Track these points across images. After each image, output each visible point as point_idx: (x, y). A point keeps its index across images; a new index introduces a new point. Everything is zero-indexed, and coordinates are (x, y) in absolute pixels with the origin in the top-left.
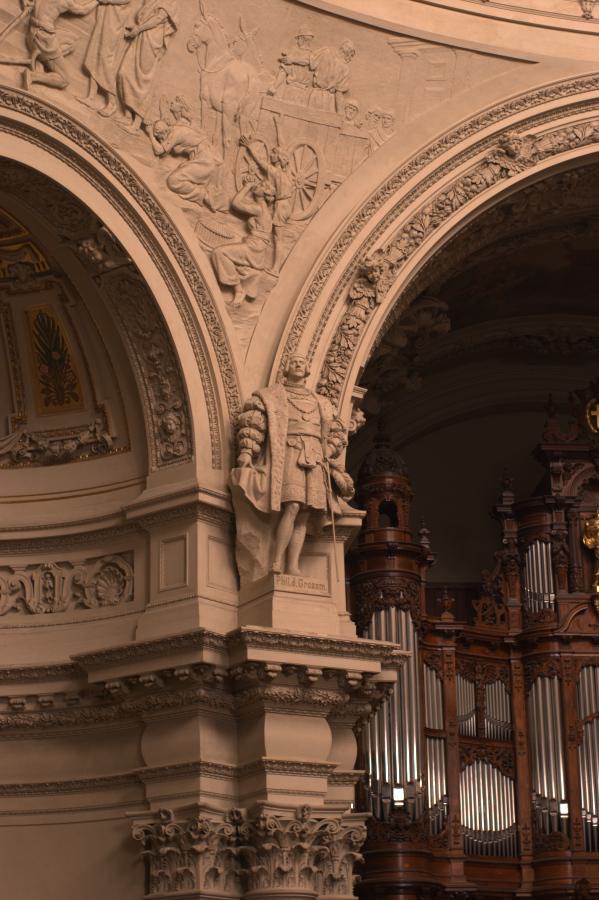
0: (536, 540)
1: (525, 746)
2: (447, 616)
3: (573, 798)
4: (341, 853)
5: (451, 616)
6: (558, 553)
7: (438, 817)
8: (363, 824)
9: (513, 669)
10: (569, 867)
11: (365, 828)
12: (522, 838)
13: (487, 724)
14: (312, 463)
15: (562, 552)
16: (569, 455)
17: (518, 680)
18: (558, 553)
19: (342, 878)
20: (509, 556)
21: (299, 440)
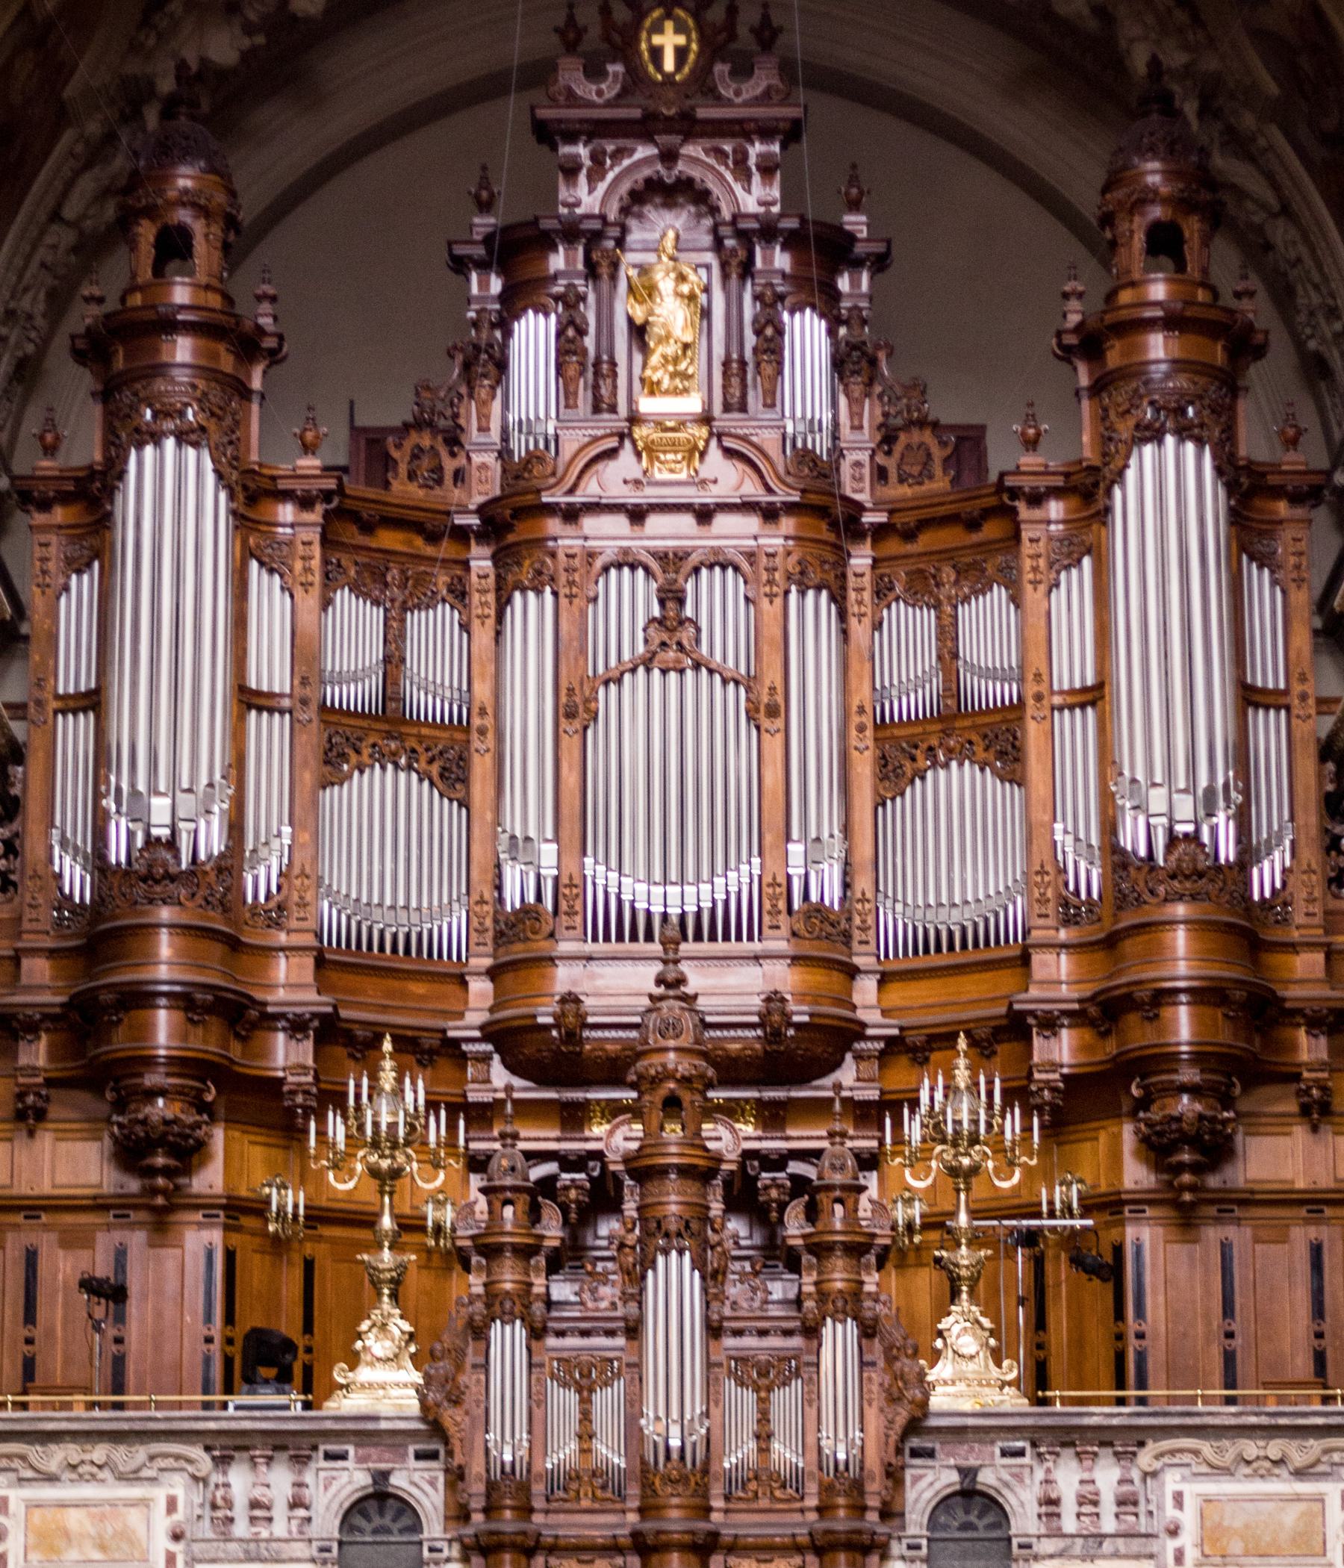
0: (524, 310)
1: (490, 735)
16: (596, 130)
17: (483, 601)
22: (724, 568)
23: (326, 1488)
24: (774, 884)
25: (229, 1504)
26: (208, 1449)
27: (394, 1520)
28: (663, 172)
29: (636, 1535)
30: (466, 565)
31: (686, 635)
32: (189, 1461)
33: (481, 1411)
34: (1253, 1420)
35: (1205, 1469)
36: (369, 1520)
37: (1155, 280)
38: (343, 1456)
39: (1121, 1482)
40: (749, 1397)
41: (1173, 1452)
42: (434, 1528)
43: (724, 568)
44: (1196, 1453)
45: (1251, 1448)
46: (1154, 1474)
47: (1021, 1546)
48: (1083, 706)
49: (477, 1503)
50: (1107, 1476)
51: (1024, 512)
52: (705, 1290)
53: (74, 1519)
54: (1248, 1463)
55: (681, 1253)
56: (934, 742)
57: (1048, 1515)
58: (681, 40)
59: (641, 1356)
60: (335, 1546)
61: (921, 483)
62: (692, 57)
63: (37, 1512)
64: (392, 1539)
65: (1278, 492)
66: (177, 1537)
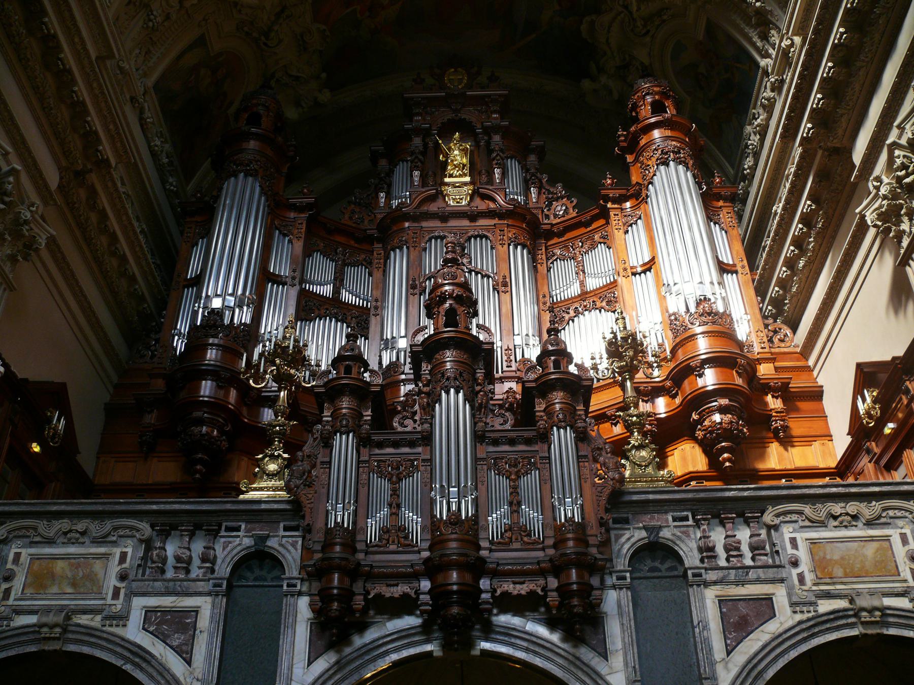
22: (481, 239)
23: (224, 549)
24: (508, 349)
25: (164, 560)
26: (152, 526)
29: (427, 561)
33: (325, 491)
35: (807, 523)
36: (253, 572)
38: (238, 529)
39: (751, 537)
40: (505, 482)
41: (785, 513)
42: (293, 570)
43: (481, 239)
44: (800, 513)
45: (837, 508)
46: (776, 527)
47: (694, 575)
48: (644, 272)
50: (744, 535)
51: (609, 205)
52: (473, 416)
53: (60, 565)
54: (835, 518)
55: (457, 392)
57: (708, 557)
59: (431, 456)
60: (225, 583)
61: (564, 216)
63: (38, 562)
64: (266, 583)
65: (718, 197)
66: (123, 577)
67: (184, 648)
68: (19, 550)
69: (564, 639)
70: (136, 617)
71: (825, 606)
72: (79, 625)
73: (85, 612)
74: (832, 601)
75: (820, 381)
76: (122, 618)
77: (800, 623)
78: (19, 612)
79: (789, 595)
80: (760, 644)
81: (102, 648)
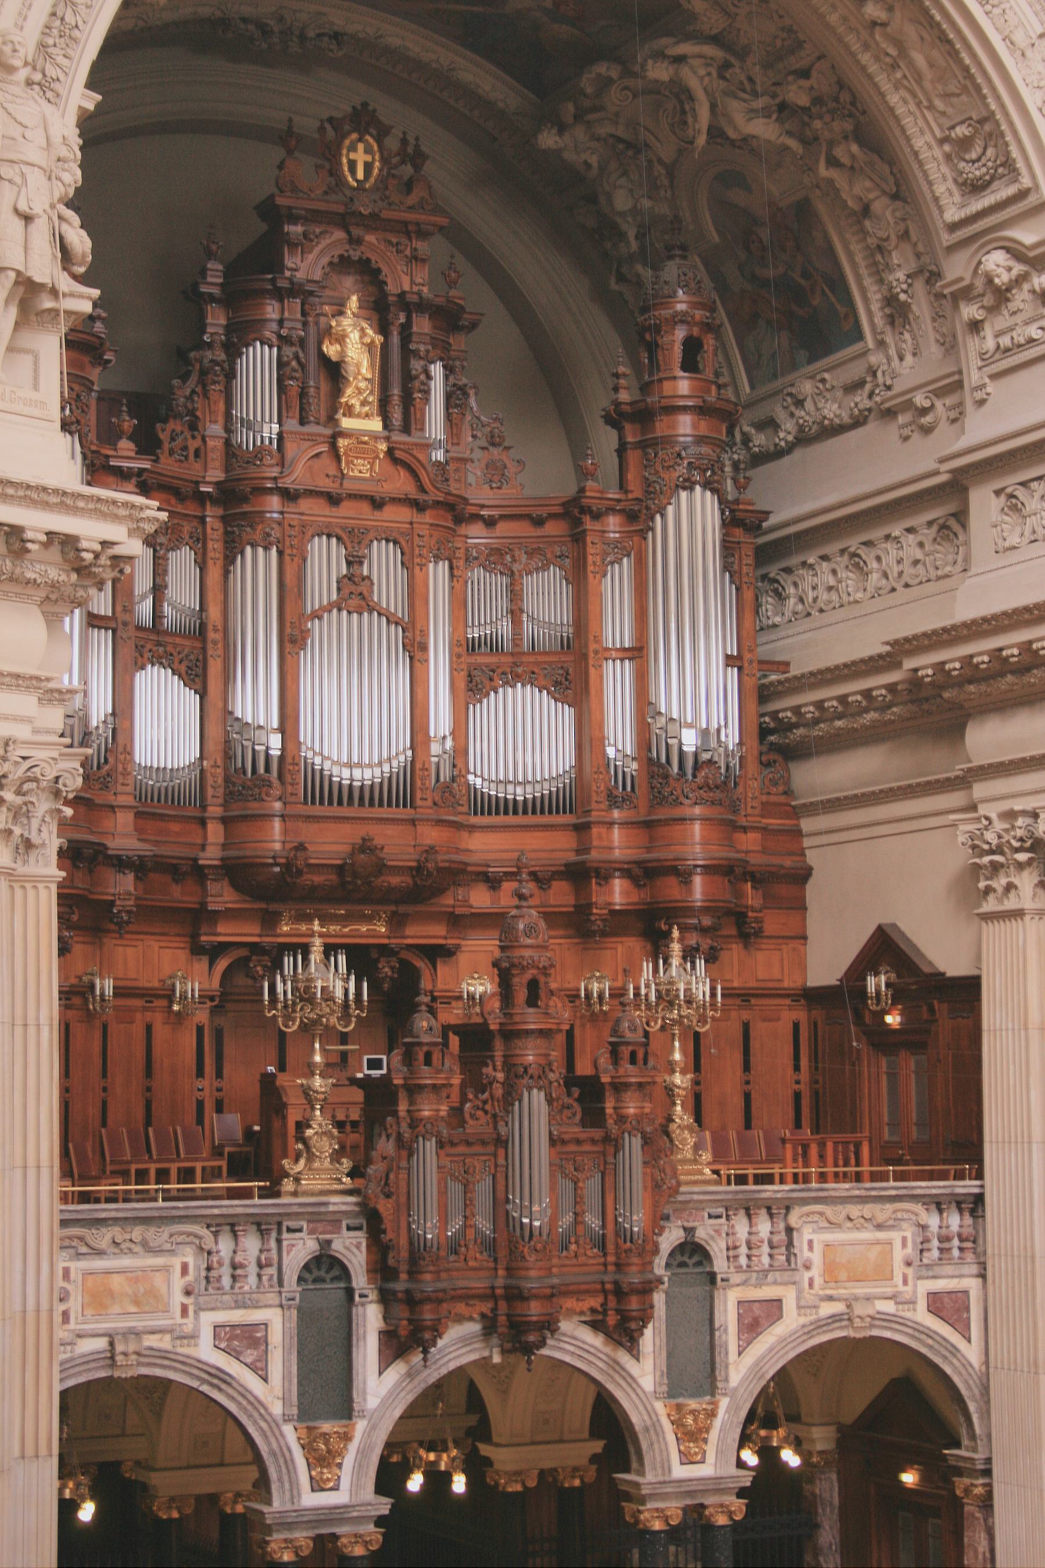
0: (254, 340)
1: (220, 645)
2: (126, 446)
3: (288, 724)
4: (43, 805)
5: (131, 445)
6: (288, 364)
7: (99, 746)
8: (77, 765)
9: (209, 531)
10: (277, 824)
11: (81, 771)
12: (210, 781)
13: (167, 609)
14: (37, 209)
15: (294, 363)
16: (314, 217)
17: (215, 547)
18: (288, 364)
19: (43, 845)
20: (212, 361)
21: (17, 170)
26: (208, 1226)
27: (327, 1272)
28: (351, 252)
30: (202, 520)
31: (363, 588)
32: (196, 1236)
34: (857, 1193)
37: (683, 378)
38: (300, 1230)
41: (808, 1215)
42: (360, 1280)
44: (821, 1214)
45: (855, 1210)
47: (723, 1280)
49: (404, 1267)
50: (764, 1227)
51: (589, 524)
56: (508, 670)
58: (369, 158)
62: (376, 171)
66: (188, 1293)
67: (259, 1364)
68: (66, 1264)
69: (606, 1344)
70: (206, 1336)
71: (827, 1309)
72: (151, 1349)
73: (153, 1333)
74: (832, 1303)
75: (812, 858)
76: (193, 1337)
77: (804, 1326)
78: (79, 1336)
79: (798, 1299)
80: (767, 1346)
81: (175, 1369)
